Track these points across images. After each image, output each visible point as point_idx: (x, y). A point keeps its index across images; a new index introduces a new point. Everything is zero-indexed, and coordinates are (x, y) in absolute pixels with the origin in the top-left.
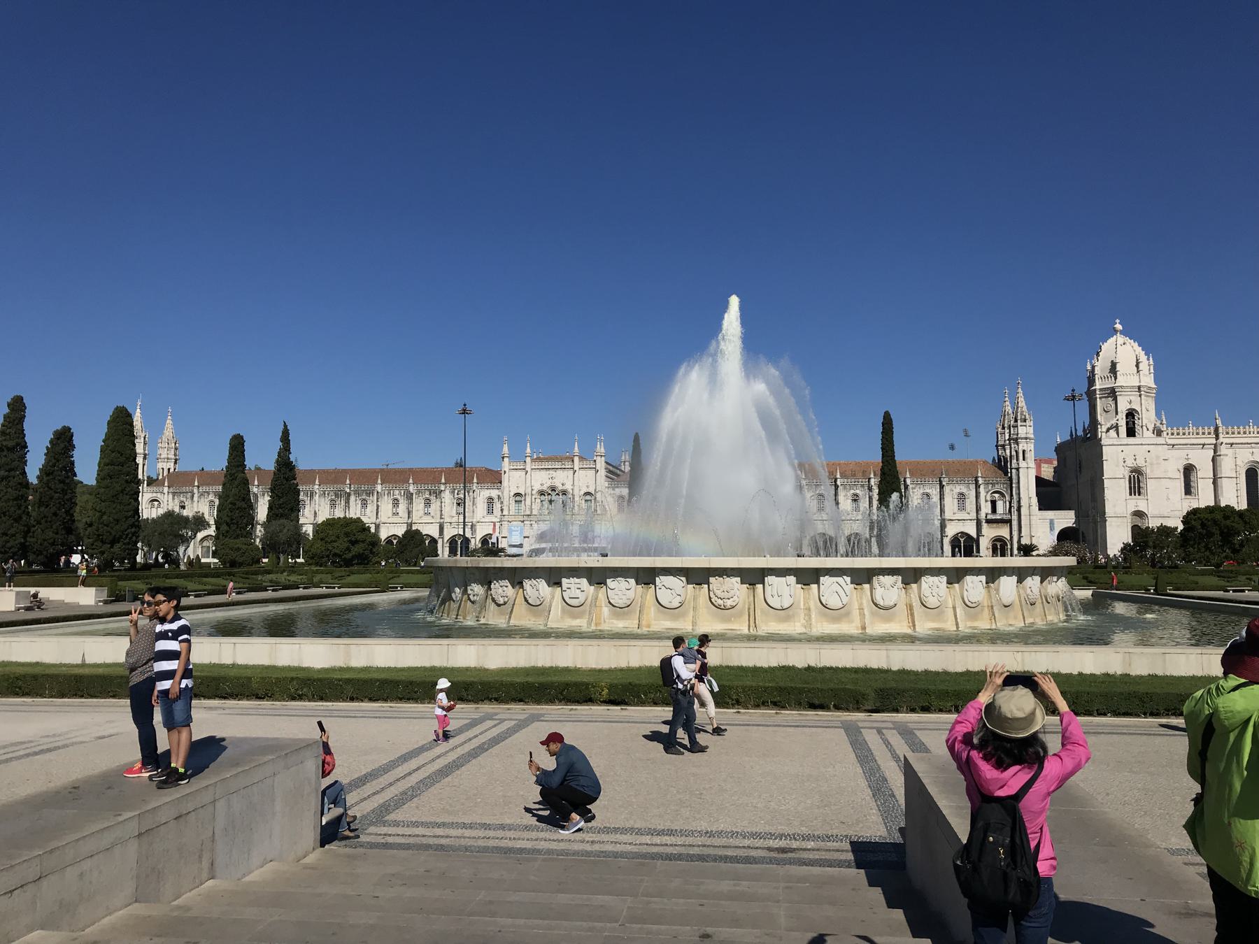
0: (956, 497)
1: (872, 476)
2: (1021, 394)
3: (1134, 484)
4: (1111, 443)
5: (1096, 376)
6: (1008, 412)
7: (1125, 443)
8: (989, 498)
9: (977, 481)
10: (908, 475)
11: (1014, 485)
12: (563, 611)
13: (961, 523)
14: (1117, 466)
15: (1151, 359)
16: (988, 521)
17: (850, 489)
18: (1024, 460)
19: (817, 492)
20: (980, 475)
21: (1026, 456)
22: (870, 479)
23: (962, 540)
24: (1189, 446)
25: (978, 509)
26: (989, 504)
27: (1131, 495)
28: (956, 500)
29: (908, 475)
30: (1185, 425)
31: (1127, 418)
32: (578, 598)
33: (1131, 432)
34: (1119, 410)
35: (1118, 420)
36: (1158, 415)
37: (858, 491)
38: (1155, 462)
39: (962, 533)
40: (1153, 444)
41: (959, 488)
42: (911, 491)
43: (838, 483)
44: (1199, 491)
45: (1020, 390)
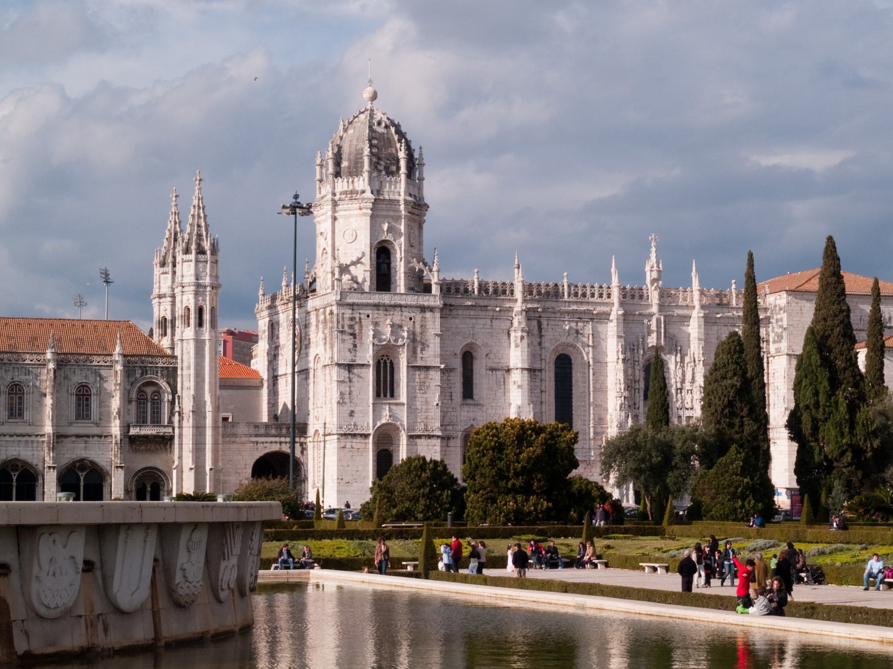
3: (385, 372)
8: (134, 395)
11: (179, 372)
18: (200, 324)
20: (118, 349)
21: (207, 317)
23: (82, 475)
27: (377, 394)
28: (74, 397)
31: (378, 257)
39: (82, 460)
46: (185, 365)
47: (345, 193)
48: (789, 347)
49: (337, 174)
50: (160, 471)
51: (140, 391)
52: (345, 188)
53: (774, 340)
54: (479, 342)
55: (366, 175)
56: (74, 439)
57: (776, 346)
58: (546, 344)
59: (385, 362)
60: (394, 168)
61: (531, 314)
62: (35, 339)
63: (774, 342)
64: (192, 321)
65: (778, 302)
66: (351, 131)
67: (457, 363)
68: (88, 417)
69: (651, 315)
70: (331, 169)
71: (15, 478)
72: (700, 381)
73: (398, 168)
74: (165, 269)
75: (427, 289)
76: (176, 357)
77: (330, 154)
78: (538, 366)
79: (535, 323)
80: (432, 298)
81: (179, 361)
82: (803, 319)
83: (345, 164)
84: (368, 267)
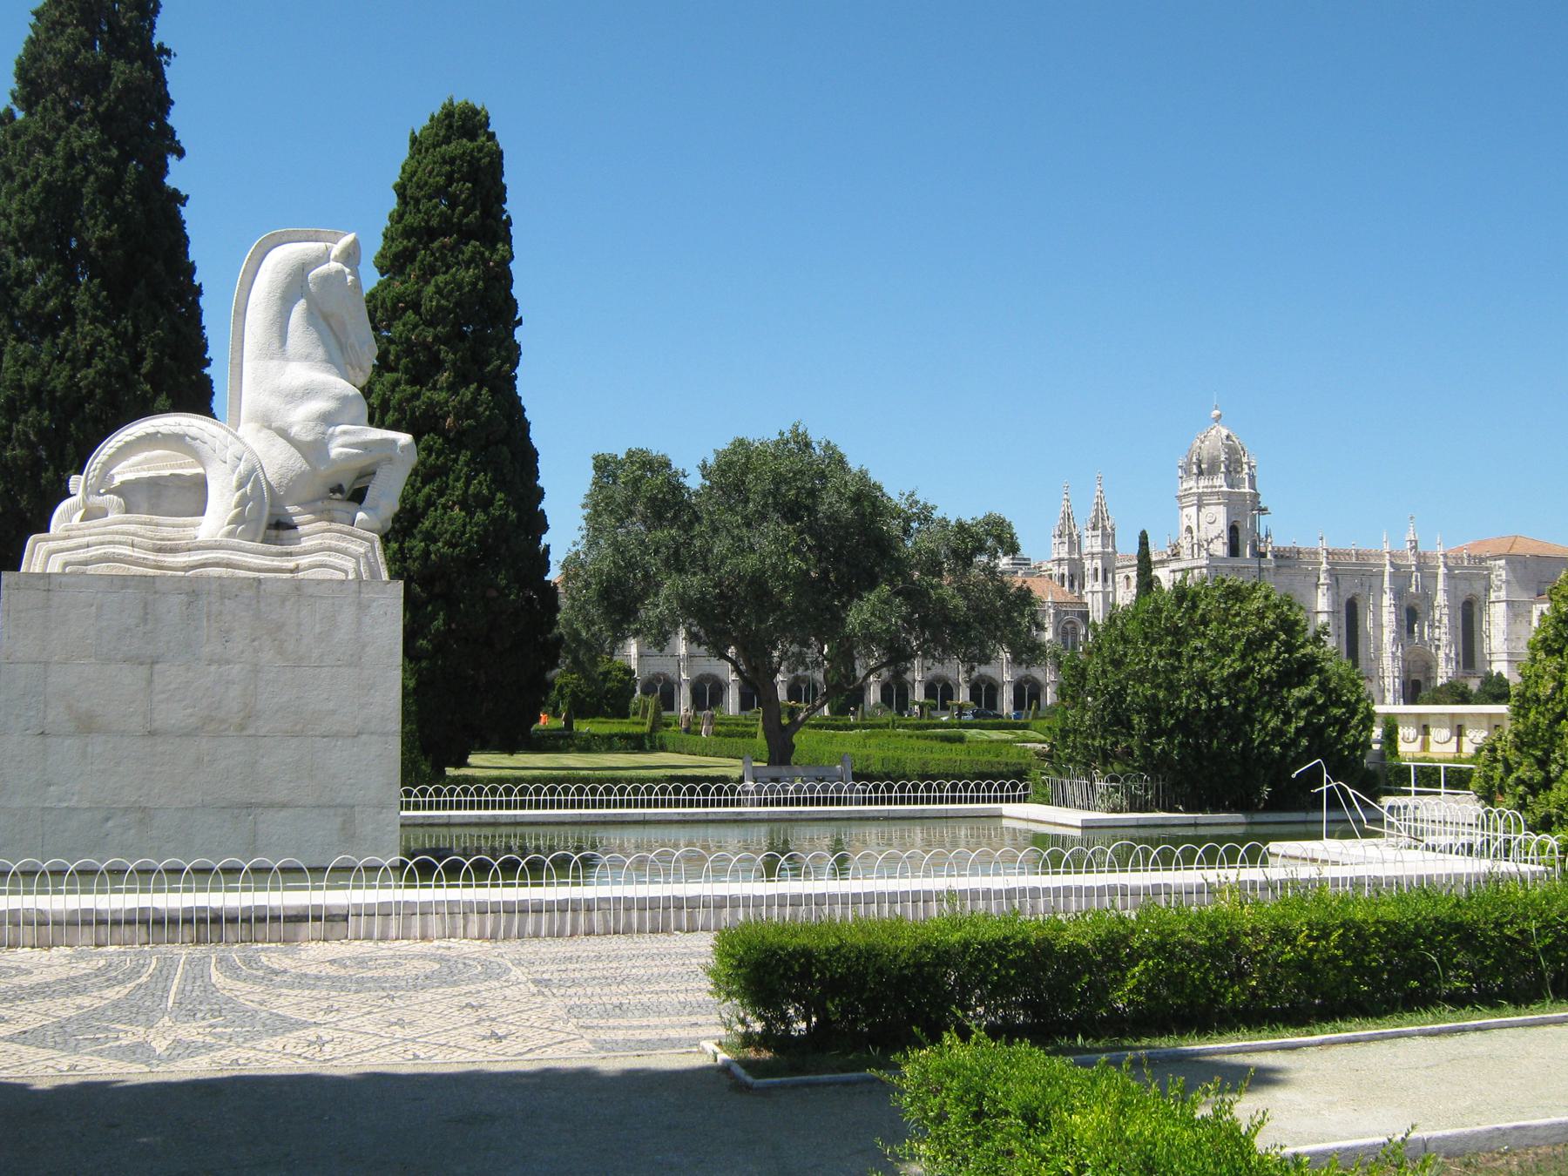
8: (1060, 630)
11: (1091, 614)
33: (1234, 549)
46: (1095, 609)
47: (1207, 487)
48: (1507, 596)
49: (1201, 473)
52: (1206, 484)
55: (1223, 475)
57: (1496, 594)
58: (1342, 593)
60: (1239, 469)
61: (1332, 572)
63: (1495, 591)
64: (1100, 578)
66: (1207, 443)
70: (1195, 470)
72: (1445, 620)
73: (1242, 469)
74: (1063, 539)
75: (1264, 555)
76: (1087, 604)
77: (1194, 460)
79: (1333, 578)
81: (1090, 606)
83: (1203, 466)
84: (1226, 540)
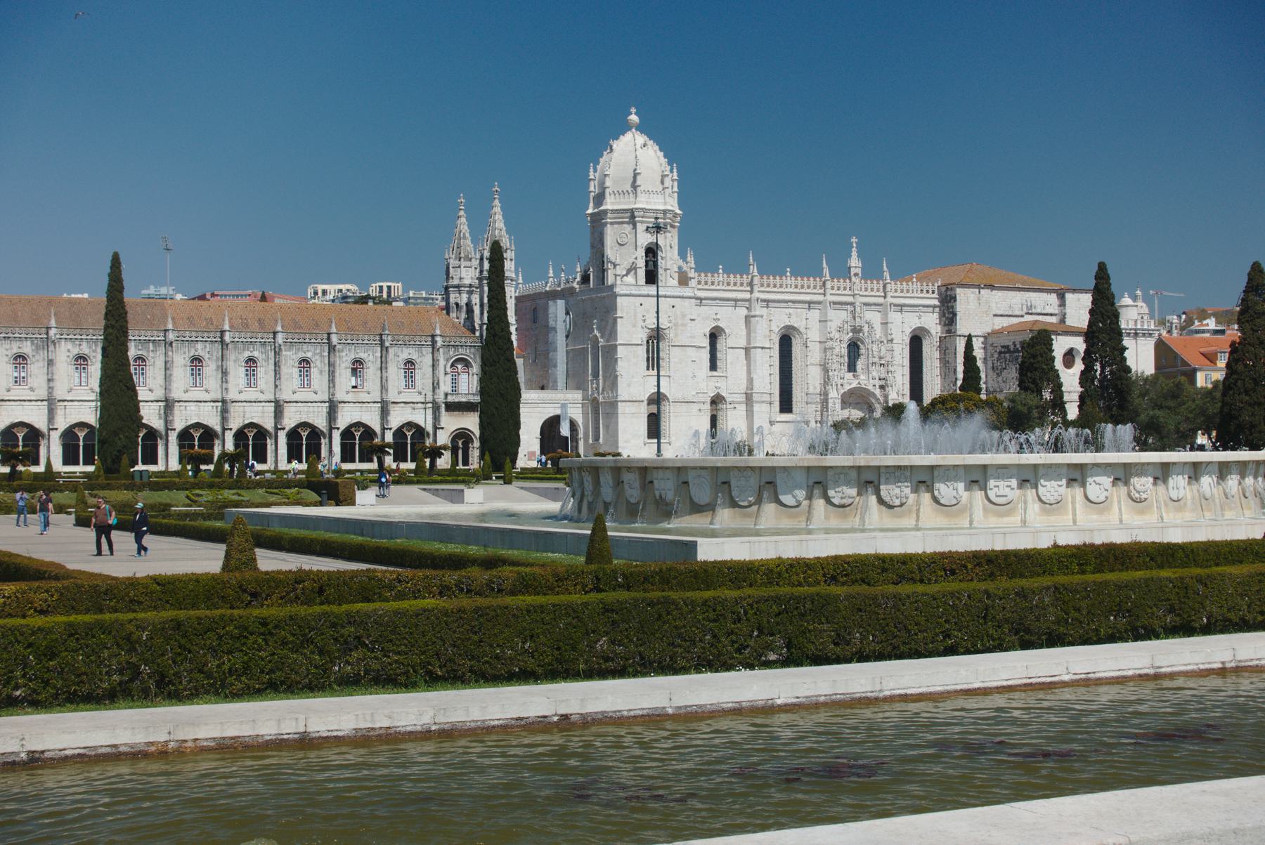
0: (402, 366)
1: (279, 328)
2: (497, 210)
4: (628, 292)
5: (607, 191)
6: (464, 234)
7: (646, 293)
8: (449, 370)
9: (434, 342)
10: (334, 330)
12: (985, 510)
13: (408, 408)
14: (634, 326)
15: (675, 170)
16: (451, 407)
17: (244, 350)
19: (192, 354)
22: (275, 333)
23: (409, 434)
24: (718, 301)
25: (436, 385)
26: (449, 377)
27: (648, 369)
28: (402, 371)
29: (334, 330)
30: (714, 271)
31: (646, 256)
32: (1006, 496)
33: (651, 278)
34: (638, 244)
35: (636, 258)
36: (683, 255)
37: (256, 354)
38: (680, 322)
40: (680, 297)
41: (406, 353)
42: (337, 354)
43: (227, 338)
44: (728, 367)
45: (497, 202)
50: (470, 431)
51: (452, 365)
53: (945, 322)
54: (721, 324)
56: (402, 405)
57: (947, 328)
59: (653, 342)
62: (366, 323)
65: (949, 293)
67: (706, 342)
68: (414, 386)
69: (852, 304)
71: (357, 438)
78: (768, 346)
80: (687, 289)
82: (969, 307)
